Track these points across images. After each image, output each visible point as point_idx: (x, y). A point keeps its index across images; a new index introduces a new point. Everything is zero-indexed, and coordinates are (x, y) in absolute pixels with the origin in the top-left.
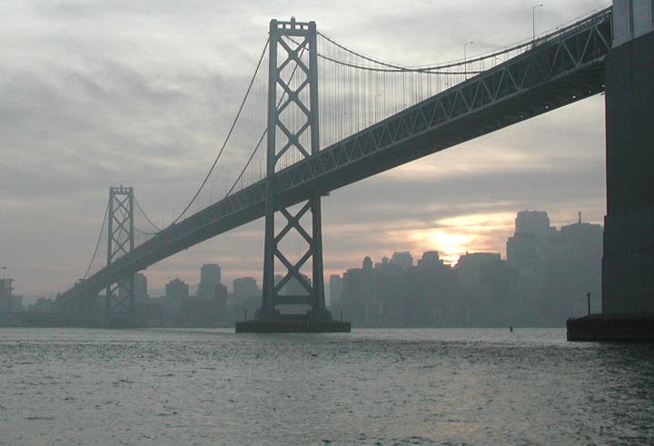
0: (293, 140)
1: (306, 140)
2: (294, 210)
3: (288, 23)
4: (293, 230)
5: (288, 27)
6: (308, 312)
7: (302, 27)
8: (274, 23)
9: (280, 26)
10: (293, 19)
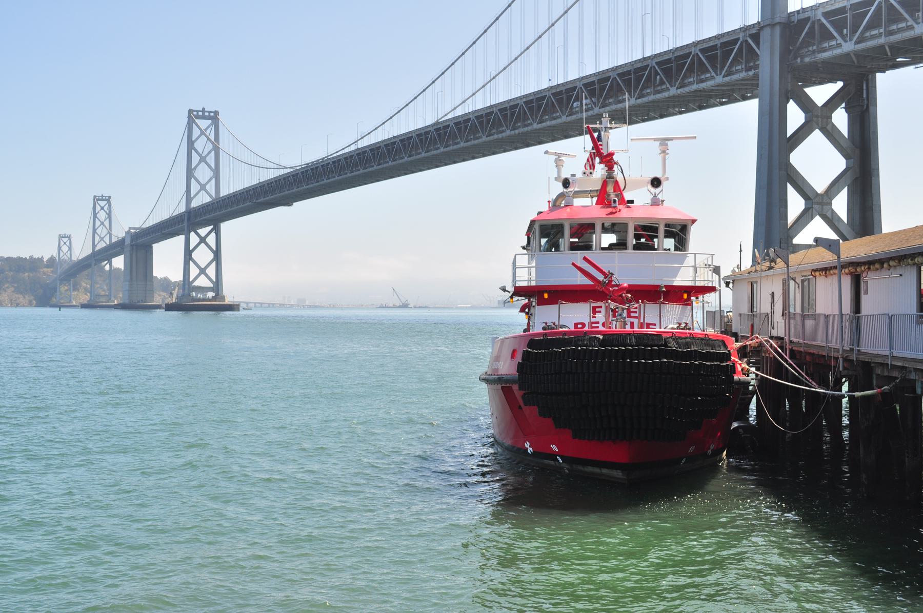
0: (203, 187)
1: (211, 188)
2: (203, 231)
3: (200, 111)
4: (203, 244)
5: (200, 113)
6: (212, 297)
7: (209, 114)
8: (191, 111)
9: (195, 113)
10: (204, 109)
